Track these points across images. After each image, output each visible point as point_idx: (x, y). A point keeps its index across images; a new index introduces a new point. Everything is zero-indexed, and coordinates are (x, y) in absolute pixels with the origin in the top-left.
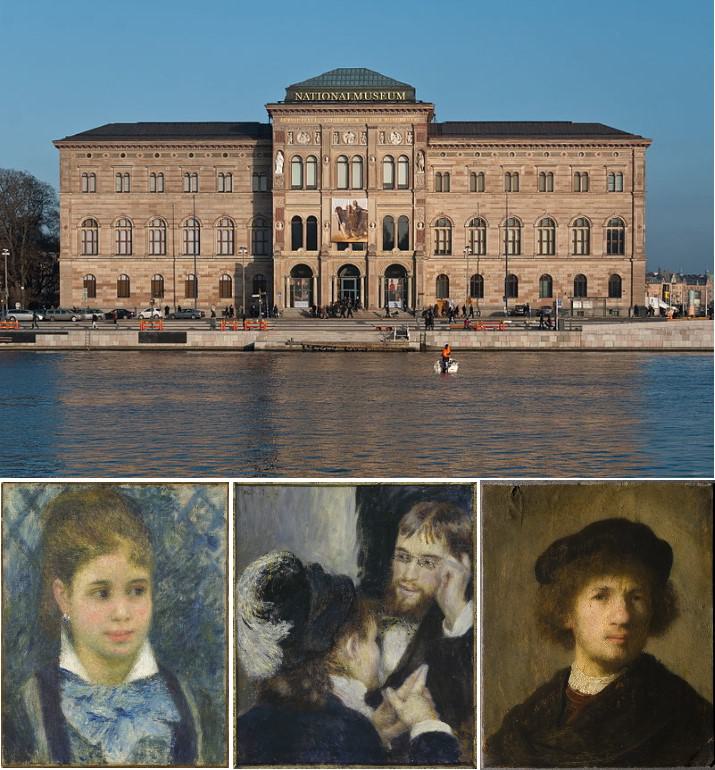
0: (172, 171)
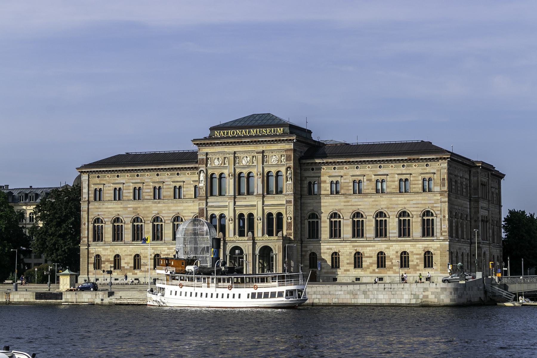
0: (146, 186)
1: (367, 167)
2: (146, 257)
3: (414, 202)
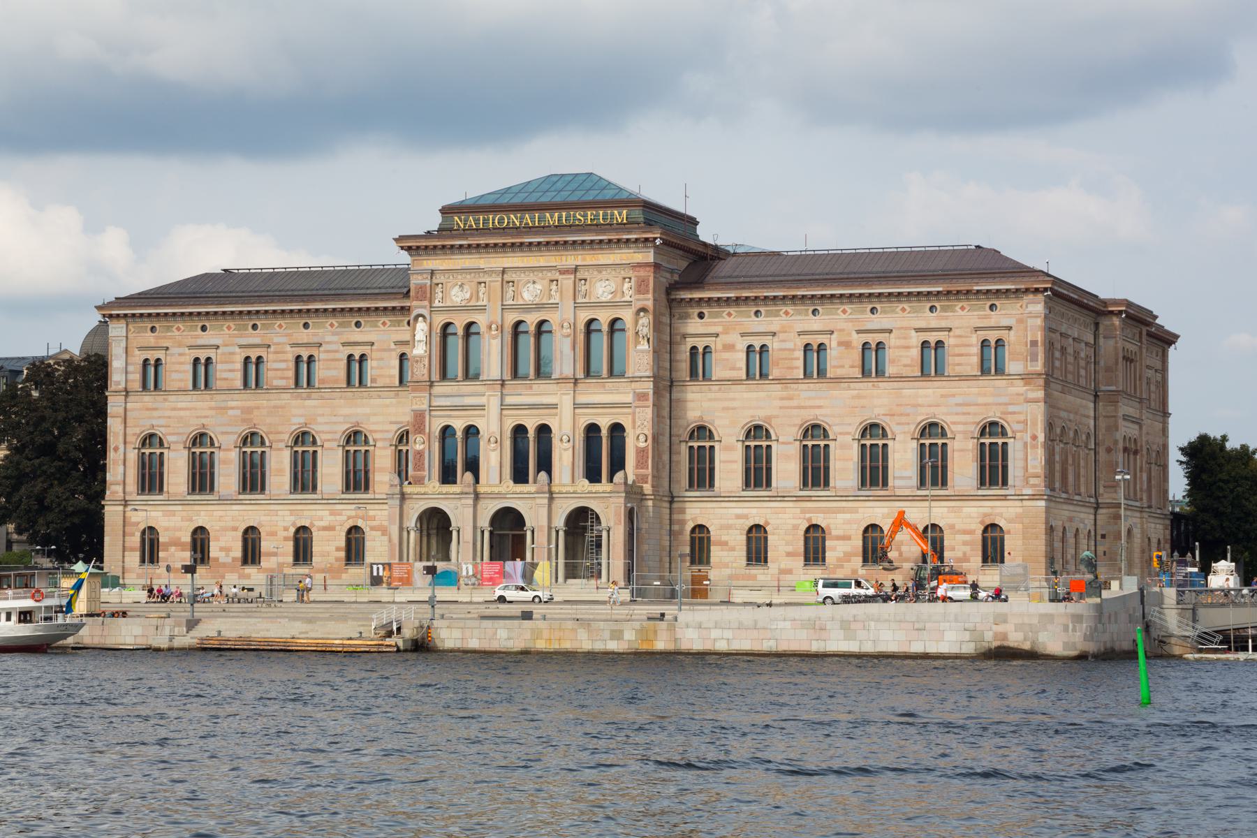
0: (276, 353)
2: (273, 534)
3: (959, 400)
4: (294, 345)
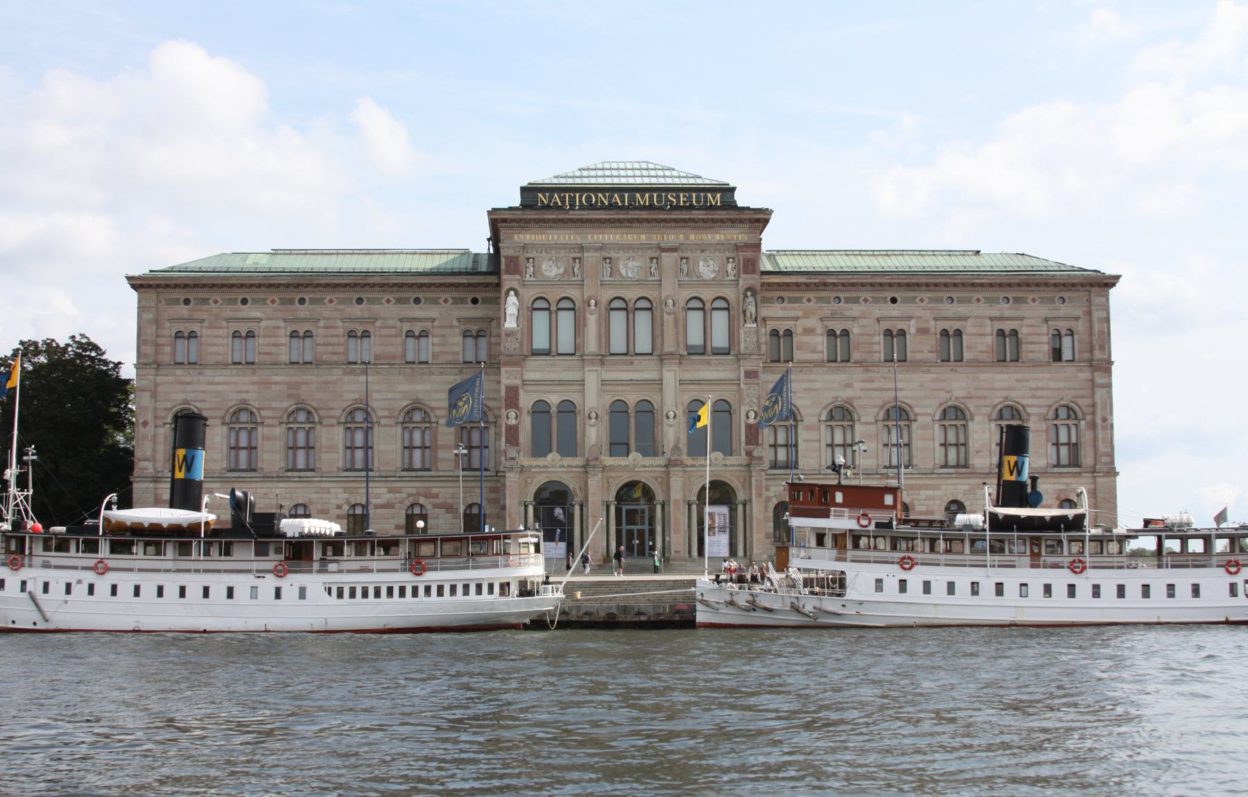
0: (326, 327)
1: (917, 300)
3: (1033, 384)
4: (351, 320)
